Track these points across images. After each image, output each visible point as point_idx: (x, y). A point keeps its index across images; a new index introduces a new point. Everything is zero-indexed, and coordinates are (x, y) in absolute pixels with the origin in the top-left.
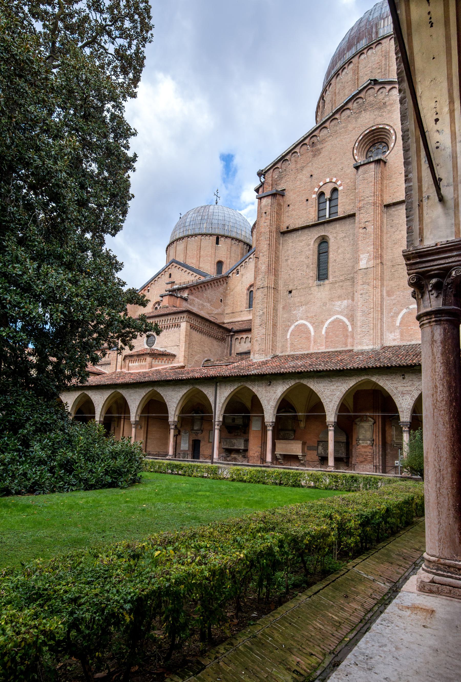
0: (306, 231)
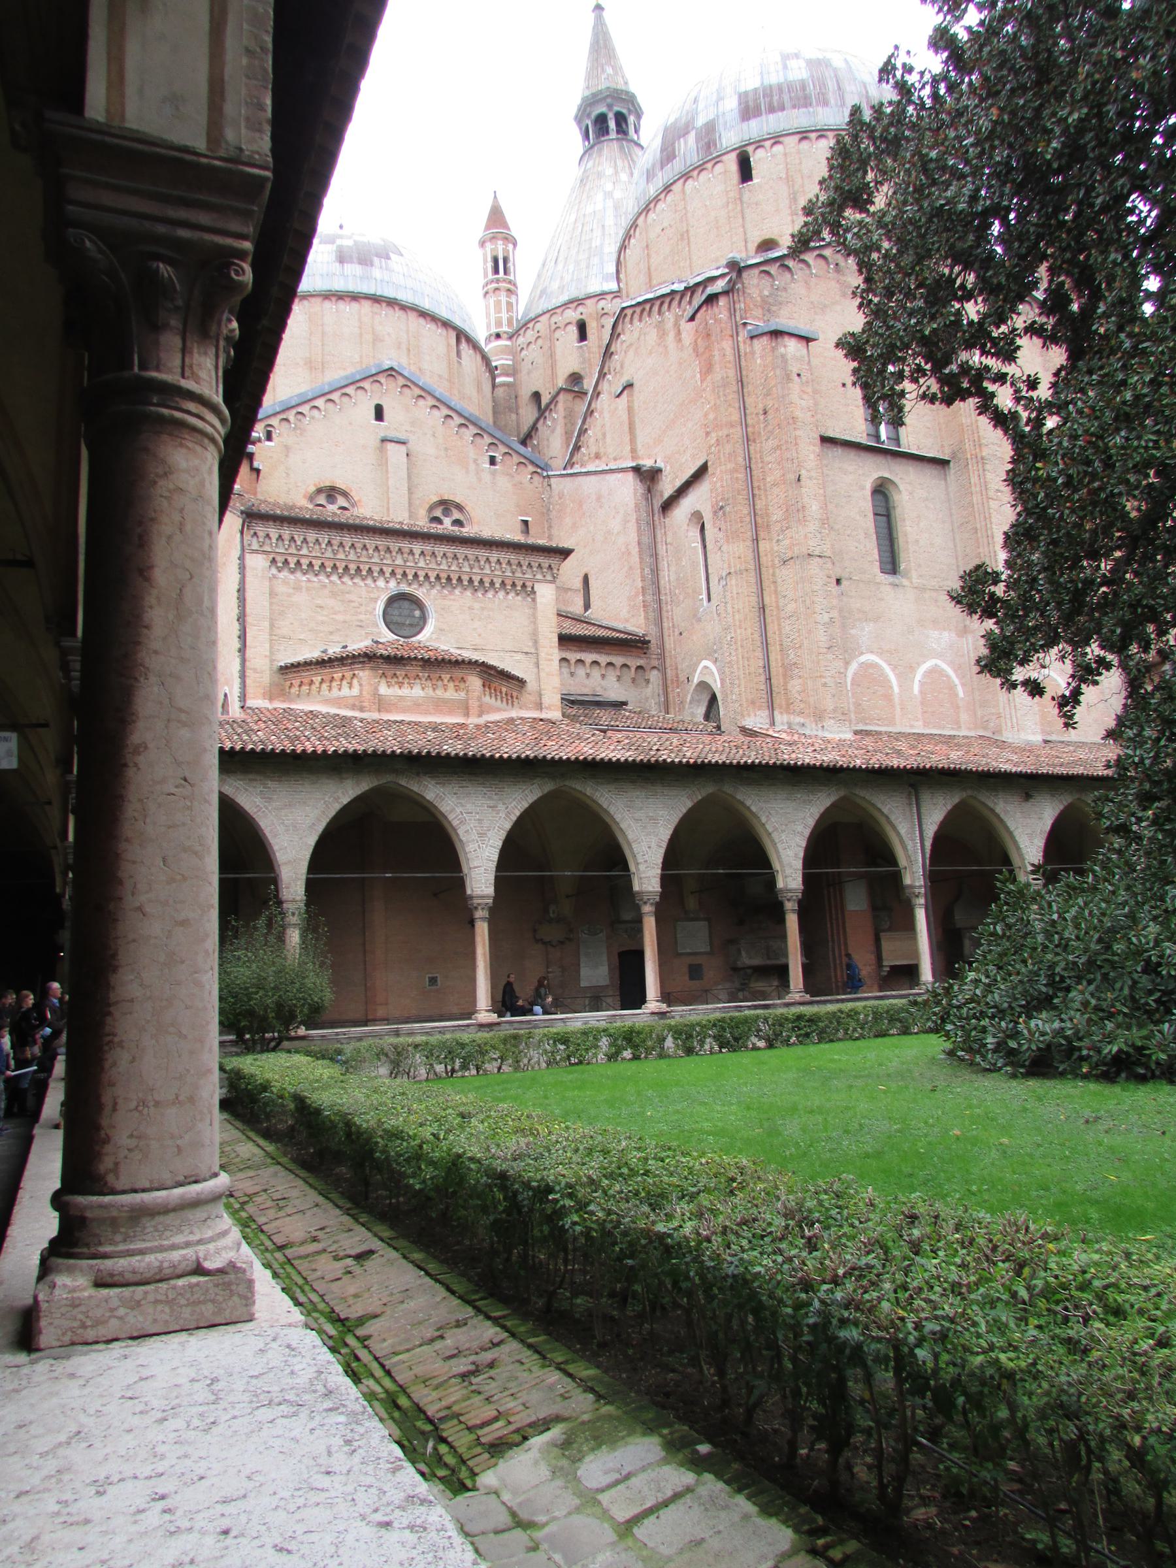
0: (852, 454)
